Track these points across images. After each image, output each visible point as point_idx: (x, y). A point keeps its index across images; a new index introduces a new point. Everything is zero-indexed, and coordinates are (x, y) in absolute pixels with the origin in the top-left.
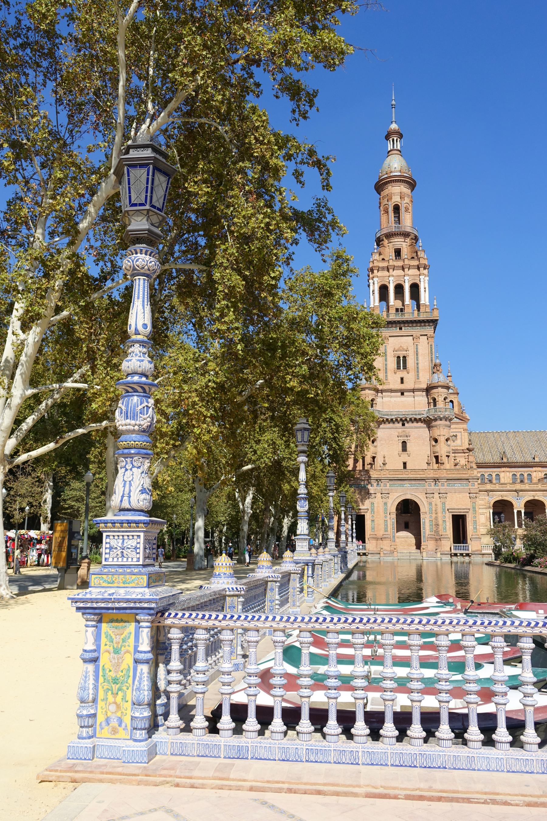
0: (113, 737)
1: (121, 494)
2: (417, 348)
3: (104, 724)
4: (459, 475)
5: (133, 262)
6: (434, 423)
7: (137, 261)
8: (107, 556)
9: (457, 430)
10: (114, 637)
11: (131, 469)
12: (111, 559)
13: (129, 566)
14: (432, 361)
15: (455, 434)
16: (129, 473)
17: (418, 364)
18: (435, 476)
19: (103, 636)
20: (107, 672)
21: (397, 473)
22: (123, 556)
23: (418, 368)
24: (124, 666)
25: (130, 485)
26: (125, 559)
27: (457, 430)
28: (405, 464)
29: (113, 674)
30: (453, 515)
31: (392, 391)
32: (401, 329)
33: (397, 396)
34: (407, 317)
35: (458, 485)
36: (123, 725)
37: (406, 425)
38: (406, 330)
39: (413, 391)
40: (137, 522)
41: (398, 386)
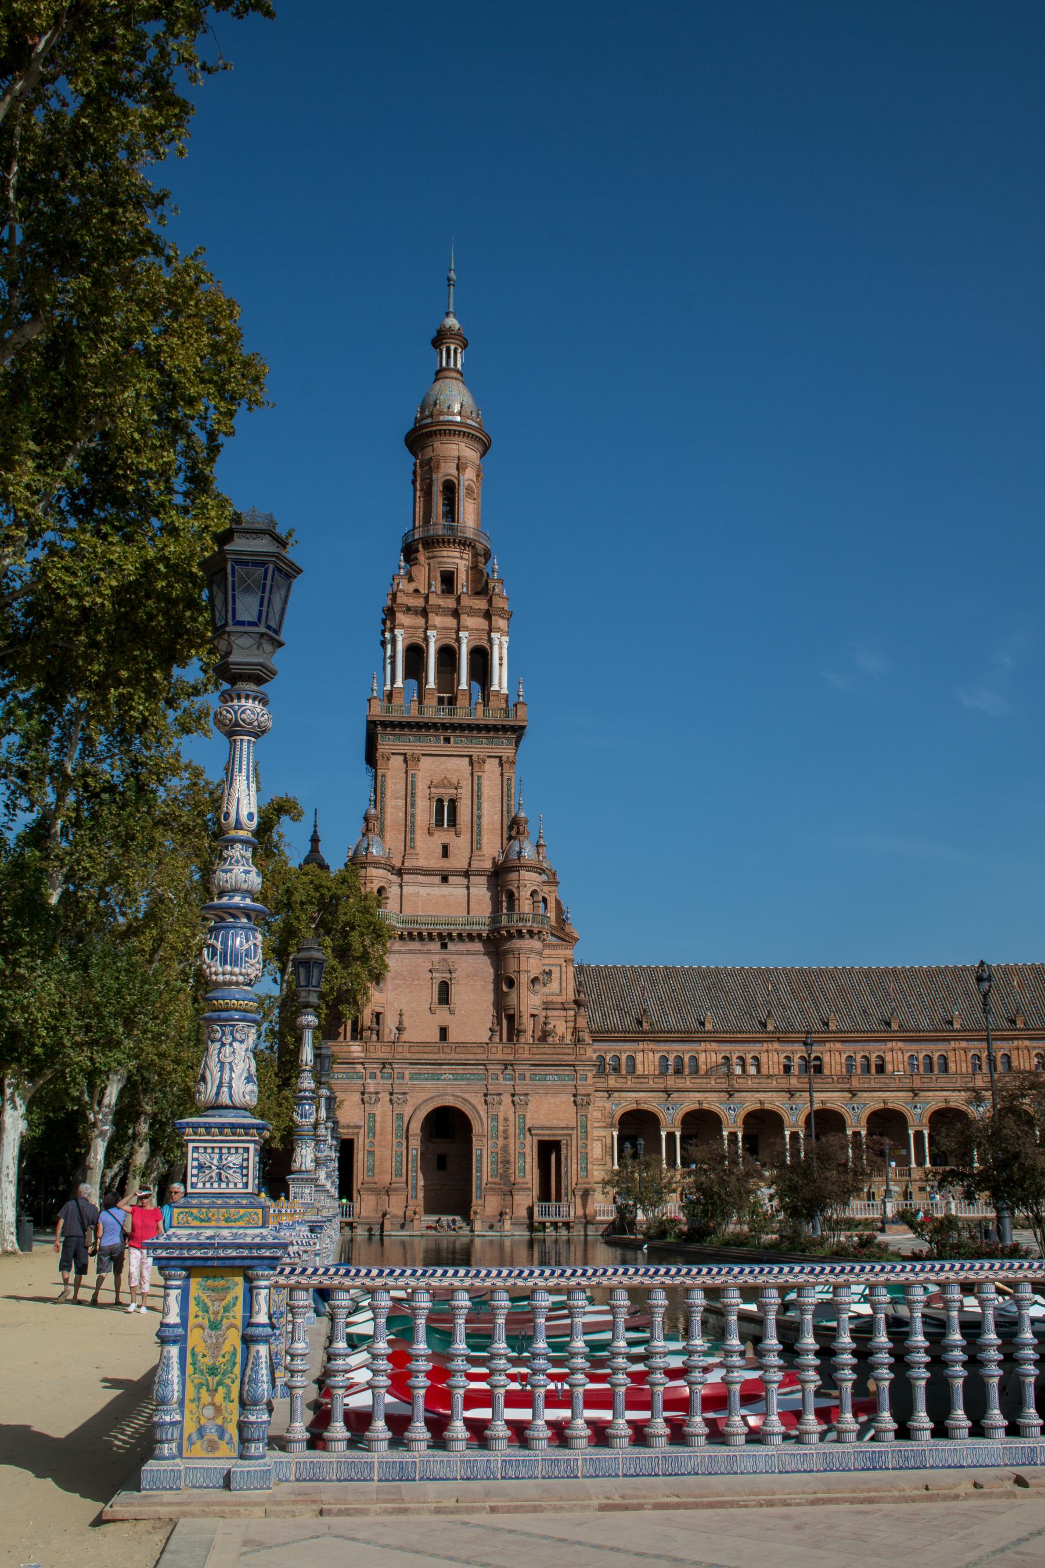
0: (211, 1455)
1: (217, 1083)
3: (195, 1437)
5: (236, 713)
7: (243, 712)
8: (194, 1180)
9: (552, 961)
10: (209, 1304)
11: (231, 1045)
12: (200, 1185)
13: (231, 1196)
16: (228, 1049)
18: (506, 1057)
19: (192, 1303)
20: (200, 1357)
21: (427, 1050)
22: (220, 1180)
24: (227, 1348)
25: (232, 1070)
26: (224, 1185)
27: (552, 961)
28: (444, 1032)
29: (208, 1361)
30: (540, 1142)
32: (447, 740)
33: (432, 885)
34: (461, 716)
35: (552, 1078)
36: (227, 1437)
37: (451, 946)
38: (460, 744)
40: (246, 1127)
41: (436, 862)
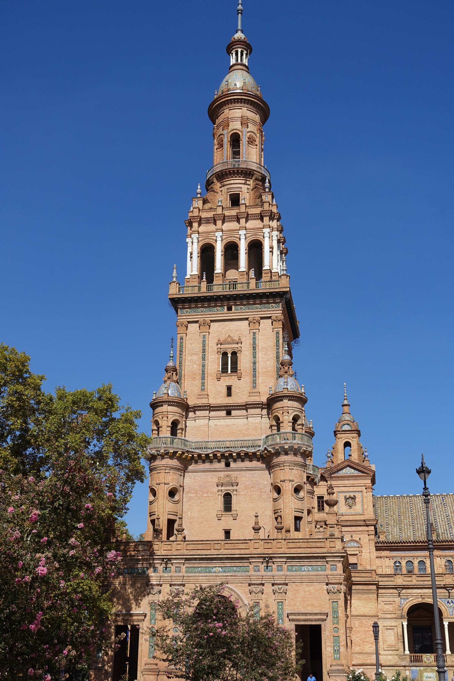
2: (254, 338)
4: (309, 550)
6: (276, 460)
9: (355, 489)
14: (278, 357)
15: (352, 495)
17: (254, 363)
18: (266, 551)
21: (200, 547)
23: (254, 369)
27: (355, 489)
28: (227, 533)
31: (210, 408)
32: (230, 309)
33: (219, 417)
35: (307, 569)
37: (232, 465)
38: (238, 311)
39: (246, 407)
